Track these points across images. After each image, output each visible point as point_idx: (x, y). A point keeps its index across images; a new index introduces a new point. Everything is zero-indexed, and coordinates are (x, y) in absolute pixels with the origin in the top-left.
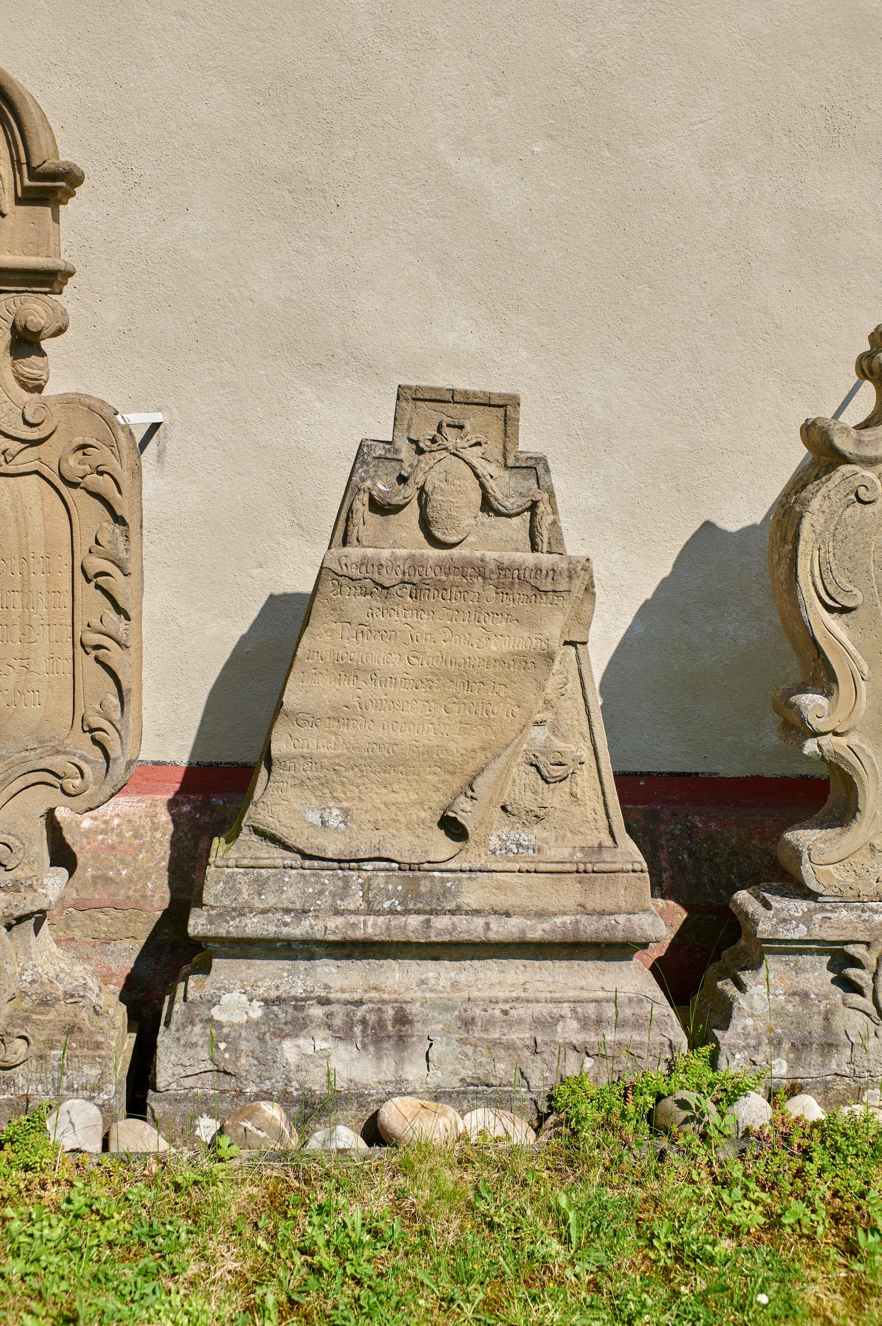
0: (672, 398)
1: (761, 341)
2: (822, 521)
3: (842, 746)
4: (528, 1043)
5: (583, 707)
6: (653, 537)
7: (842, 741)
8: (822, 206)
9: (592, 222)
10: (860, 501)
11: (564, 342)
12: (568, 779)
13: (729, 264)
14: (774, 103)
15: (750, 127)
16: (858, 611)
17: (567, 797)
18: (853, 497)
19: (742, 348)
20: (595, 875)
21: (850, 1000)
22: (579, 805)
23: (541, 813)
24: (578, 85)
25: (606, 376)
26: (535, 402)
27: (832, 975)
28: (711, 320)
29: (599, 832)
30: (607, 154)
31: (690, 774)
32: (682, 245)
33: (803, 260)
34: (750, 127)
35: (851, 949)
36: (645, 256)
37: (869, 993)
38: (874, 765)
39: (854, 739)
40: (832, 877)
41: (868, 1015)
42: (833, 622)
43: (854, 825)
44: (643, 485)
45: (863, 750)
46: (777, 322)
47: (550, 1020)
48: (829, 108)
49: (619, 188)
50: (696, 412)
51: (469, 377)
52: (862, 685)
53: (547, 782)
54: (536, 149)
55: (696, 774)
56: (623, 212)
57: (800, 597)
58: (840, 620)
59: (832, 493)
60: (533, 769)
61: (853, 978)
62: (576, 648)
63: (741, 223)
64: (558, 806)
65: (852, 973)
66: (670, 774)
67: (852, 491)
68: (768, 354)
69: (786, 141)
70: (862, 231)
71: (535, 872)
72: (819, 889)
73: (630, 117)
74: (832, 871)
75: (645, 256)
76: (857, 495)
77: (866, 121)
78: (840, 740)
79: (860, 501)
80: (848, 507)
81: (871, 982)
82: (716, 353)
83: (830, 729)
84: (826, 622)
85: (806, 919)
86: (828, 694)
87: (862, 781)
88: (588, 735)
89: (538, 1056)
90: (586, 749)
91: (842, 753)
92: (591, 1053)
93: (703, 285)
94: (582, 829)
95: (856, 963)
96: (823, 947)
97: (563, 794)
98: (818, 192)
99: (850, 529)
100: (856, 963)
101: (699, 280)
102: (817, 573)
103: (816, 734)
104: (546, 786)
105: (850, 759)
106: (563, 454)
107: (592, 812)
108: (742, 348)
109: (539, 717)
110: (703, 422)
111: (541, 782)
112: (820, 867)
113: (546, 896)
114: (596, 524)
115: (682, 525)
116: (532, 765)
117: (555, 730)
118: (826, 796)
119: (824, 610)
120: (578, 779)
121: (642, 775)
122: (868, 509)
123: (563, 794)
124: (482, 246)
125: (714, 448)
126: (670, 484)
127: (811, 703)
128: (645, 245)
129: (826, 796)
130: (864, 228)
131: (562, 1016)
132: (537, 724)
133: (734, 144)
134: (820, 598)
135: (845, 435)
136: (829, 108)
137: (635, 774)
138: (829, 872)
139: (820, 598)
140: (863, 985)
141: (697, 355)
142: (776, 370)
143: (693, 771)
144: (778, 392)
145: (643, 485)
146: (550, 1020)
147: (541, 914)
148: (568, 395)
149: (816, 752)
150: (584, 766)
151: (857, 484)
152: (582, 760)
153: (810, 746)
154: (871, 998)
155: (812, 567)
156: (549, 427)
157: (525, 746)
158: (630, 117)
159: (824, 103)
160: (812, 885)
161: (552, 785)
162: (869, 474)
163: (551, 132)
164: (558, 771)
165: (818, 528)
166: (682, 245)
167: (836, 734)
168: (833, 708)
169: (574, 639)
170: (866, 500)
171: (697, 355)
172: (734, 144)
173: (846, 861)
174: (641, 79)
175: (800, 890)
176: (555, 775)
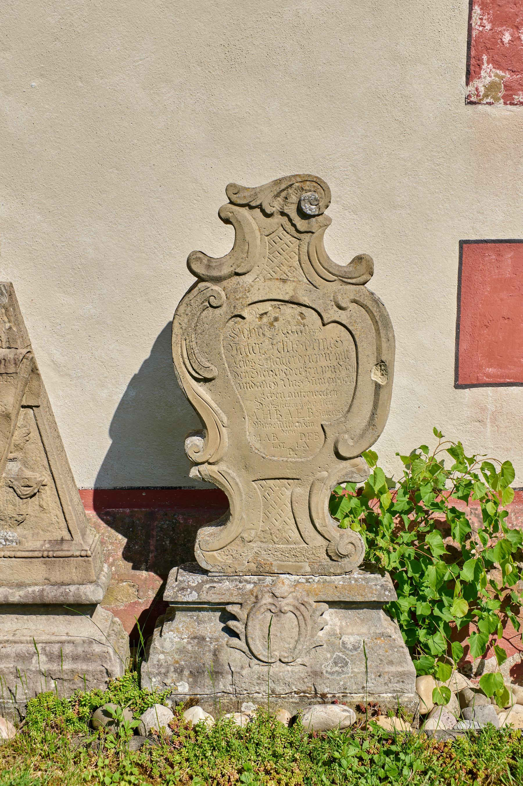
0: (139, 242)
1: (195, 202)
2: (186, 320)
3: (214, 472)
4: (12, 670)
6: (136, 333)
7: (214, 468)
8: (227, 110)
9: (75, 129)
11: (64, 208)
12: (37, 496)
13: (168, 152)
14: (189, 45)
15: (174, 61)
16: (216, 380)
17: (37, 508)
18: (207, 304)
20: (55, 559)
21: (230, 642)
22: (46, 513)
23: (20, 518)
24: (57, 40)
26: (48, 248)
27: (223, 625)
28: (160, 189)
29: (61, 531)
30: (80, 84)
31: (176, 488)
32: (135, 141)
33: (219, 147)
34: (174, 61)
35: (229, 608)
36: (112, 149)
37: (243, 637)
38: (237, 484)
39: (222, 467)
40: (216, 559)
42: (200, 389)
43: (229, 524)
44: (125, 300)
45: (229, 474)
46: (205, 188)
47: (27, 655)
48: (226, 45)
49: (90, 106)
50: (156, 250)
51: (4, 234)
52: (224, 430)
53: (21, 498)
54: (34, 84)
55: (180, 487)
58: (205, 387)
59: (192, 301)
60: (11, 490)
61: (232, 628)
63: (174, 125)
65: (232, 623)
67: (206, 300)
69: (199, 69)
70: (256, 125)
71: (15, 557)
72: (208, 568)
75: (112, 149)
77: (252, 52)
78: (213, 467)
80: (204, 310)
81: (244, 630)
82: (166, 211)
83: (204, 460)
85: (198, 588)
86: (203, 437)
88: (47, 467)
91: (215, 476)
92: (54, 677)
93: (153, 167)
94: (49, 529)
95: (234, 618)
96: (213, 607)
97: (34, 506)
98: (224, 101)
99: (205, 325)
100: (234, 618)
101: (150, 164)
102: (185, 356)
103: (197, 464)
105: (220, 480)
106: (70, 281)
109: (11, 456)
111: (17, 498)
112: (207, 553)
113: (22, 573)
115: (154, 325)
116: (10, 487)
117: (25, 463)
118: (213, 505)
119: (193, 381)
120: (43, 496)
121: (143, 489)
122: (217, 311)
123: (34, 506)
124: (4, 149)
125: (170, 273)
128: (111, 142)
129: (213, 505)
132: (11, 460)
133: (165, 73)
134: (189, 372)
135: (199, 262)
136: (226, 45)
137: (139, 488)
139: (189, 372)
141: (153, 213)
142: (207, 220)
143: (178, 485)
144: (211, 234)
145: (125, 300)
146: (27, 655)
147: (20, 585)
148: (70, 243)
149: (197, 476)
151: (208, 295)
152: (44, 483)
153: (194, 472)
154: (244, 641)
155: (182, 352)
156: (60, 264)
157: (4, 475)
159: (223, 42)
160: (203, 565)
161: (25, 500)
163: (43, 73)
164: (27, 491)
165: (184, 325)
166: (135, 141)
167: (210, 464)
168: (206, 445)
169: (30, 404)
170: (215, 305)
171: (153, 213)
172: (165, 73)
173: (226, 548)
174: (98, 34)
176: (25, 493)
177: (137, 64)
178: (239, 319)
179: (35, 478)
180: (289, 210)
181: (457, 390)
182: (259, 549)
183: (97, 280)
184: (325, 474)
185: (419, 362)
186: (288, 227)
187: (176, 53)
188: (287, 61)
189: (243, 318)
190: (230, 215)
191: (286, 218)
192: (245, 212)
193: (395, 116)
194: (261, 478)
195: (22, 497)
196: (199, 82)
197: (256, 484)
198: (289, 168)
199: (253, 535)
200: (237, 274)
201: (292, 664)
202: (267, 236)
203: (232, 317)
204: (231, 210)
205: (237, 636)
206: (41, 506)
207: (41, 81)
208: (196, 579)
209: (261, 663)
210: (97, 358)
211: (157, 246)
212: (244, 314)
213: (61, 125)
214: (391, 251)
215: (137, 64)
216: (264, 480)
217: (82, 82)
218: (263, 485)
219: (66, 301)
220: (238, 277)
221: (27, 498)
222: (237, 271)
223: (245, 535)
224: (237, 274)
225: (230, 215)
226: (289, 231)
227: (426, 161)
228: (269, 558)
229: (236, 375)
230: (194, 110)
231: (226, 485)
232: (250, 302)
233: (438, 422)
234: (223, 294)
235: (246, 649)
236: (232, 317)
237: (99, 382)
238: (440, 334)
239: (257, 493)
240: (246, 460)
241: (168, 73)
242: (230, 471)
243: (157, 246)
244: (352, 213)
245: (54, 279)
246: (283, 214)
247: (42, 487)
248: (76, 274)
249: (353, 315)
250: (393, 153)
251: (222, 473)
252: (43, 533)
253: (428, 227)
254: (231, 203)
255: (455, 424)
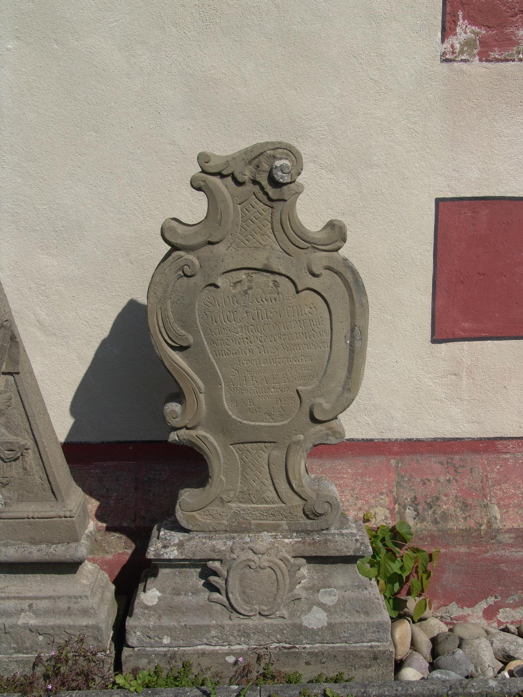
1: (173, 163)
2: (161, 290)
3: (192, 436)
5: (23, 413)
7: (193, 433)
10: (186, 275)
12: (20, 459)
13: (146, 114)
14: (163, 5)
16: (192, 348)
17: (21, 470)
18: (181, 273)
19: (162, 168)
21: (211, 597)
22: (30, 475)
23: (5, 481)
25: (74, 192)
26: (30, 211)
27: (203, 581)
28: (138, 152)
29: (46, 492)
30: (56, 47)
31: (161, 441)
32: (113, 104)
33: (196, 108)
36: (89, 112)
37: (224, 592)
38: (215, 448)
40: (196, 519)
41: (225, 606)
42: (176, 356)
44: (107, 261)
46: (183, 150)
48: (201, 5)
49: (67, 69)
50: (136, 212)
52: (202, 397)
54: (9, 46)
56: (71, 85)
57: (153, 341)
61: (213, 583)
62: (14, 377)
63: (151, 87)
64: (16, 476)
65: (213, 579)
66: (141, 442)
67: (179, 270)
68: (179, 171)
69: (174, 30)
70: (233, 86)
72: (190, 527)
73: (68, 21)
74: (197, 516)
75: (89, 112)
76: (183, 272)
77: (227, 13)
79: (186, 275)
81: (224, 585)
83: (182, 426)
84: (172, 357)
86: (181, 403)
87: (209, 458)
88: (30, 431)
89: (7, 635)
90: (30, 440)
91: (193, 441)
92: (41, 632)
95: (215, 573)
97: (18, 468)
98: (200, 62)
100: (215, 573)
101: (128, 126)
102: (161, 324)
103: (175, 429)
104: (5, 464)
106: (53, 243)
107: (39, 479)
108: (162, 168)
110: (142, 218)
112: (188, 513)
114: (80, 287)
120: (27, 459)
121: (130, 442)
122: (192, 280)
123: (18, 468)
125: (151, 234)
126: (125, 259)
127: (174, 407)
128: (88, 105)
130: (234, 84)
131: (22, 610)
133: (140, 35)
136: (201, 5)
137: (125, 442)
138: (193, 516)
140: (220, 587)
143: (163, 439)
144: (190, 195)
145: (107, 261)
148: (51, 206)
149: (176, 440)
150: (30, 451)
152: (26, 447)
154: (225, 595)
155: (157, 320)
156: (42, 227)
158: (68, 21)
161: (9, 464)
162: (191, 257)
163: (18, 35)
164: (10, 455)
165: (158, 293)
166: (113, 104)
167: (188, 429)
168: (184, 411)
170: (189, 274)
172: (140, 35)
173: (206, 508)
175: (178, 528)
177: (112, 25)
178: (213, 288)
179: (18, 443)
180: (261, 179)
181: (433, 345)
182: (238, 509)
183: (79, 242)
184: (301, 437)
185: (396, 318)
186: (260, 195)
187: (150, 14)
188: (262, 21)
189: (217, 287)
190: (202, 184)
191: (257, 187)
192: (216, 180)
193: (371, 75)
194: (238, 442)
195: (6, 460)
196: (175, 44)
197: (234, 448)
198: (266, 128)
199: (232, 496)
200: (210, 243)
201: (271, 616)
202: (239, 204)
203: (206, 286)
204: (203, 179)
205: (218, 590)
206: (25, 469)
207: (16, 43)
208: (177, 537)
209: (242, 617)
210: (82, 318)
211: (137, 208)
212: (219, 284)
213: (39, 88)
214: (368, 209)
215: (112, 25)
216: (242, 443)
217: (57, 44)
218: (240, 449)
219: (50, 263)
220: (211, 246)
221: (10, 461)
222: (210, 240)
223: (224, 497)
224: (210, 243)
225: (202, 184)
226: (261, 199)
227: (402, 119)
228: (248, 518)
229: (212, 342)
230: (170, 72)
231: (204, 449)
232: (225, 271)
233: (415, 376)
234: (197, 262)
235: (227, 603)
236: (206, 286)
237: (85, 341)
238: (417, 290)
239: (235, 456)
240: (222, 424)
241: (143, 35)
242: (208, 436)
243: (137, 208)
244: (329, 172)
245: (37, 241)
246: (255, 182)
247: (25, 451)
248: (58, 236)
249: (326, 282)
250: (369, 112)
251: (201, 437)
252: (27, 494)
253: (404, 186)
254: (203, 171)
255: (432, 377)
